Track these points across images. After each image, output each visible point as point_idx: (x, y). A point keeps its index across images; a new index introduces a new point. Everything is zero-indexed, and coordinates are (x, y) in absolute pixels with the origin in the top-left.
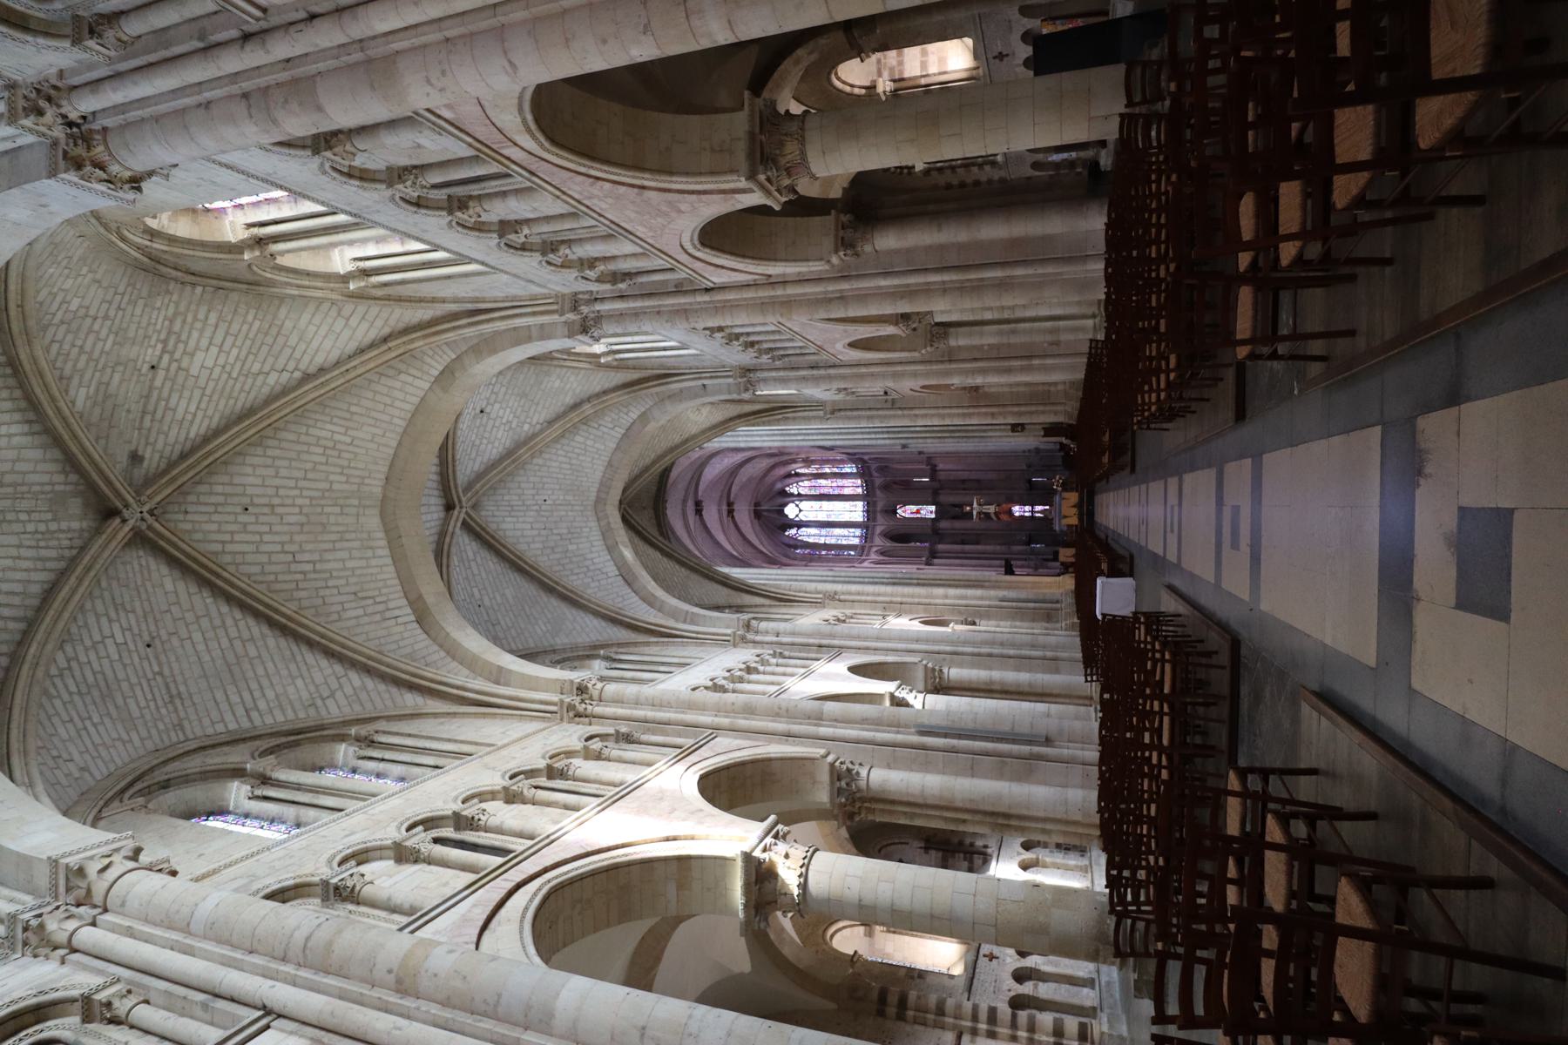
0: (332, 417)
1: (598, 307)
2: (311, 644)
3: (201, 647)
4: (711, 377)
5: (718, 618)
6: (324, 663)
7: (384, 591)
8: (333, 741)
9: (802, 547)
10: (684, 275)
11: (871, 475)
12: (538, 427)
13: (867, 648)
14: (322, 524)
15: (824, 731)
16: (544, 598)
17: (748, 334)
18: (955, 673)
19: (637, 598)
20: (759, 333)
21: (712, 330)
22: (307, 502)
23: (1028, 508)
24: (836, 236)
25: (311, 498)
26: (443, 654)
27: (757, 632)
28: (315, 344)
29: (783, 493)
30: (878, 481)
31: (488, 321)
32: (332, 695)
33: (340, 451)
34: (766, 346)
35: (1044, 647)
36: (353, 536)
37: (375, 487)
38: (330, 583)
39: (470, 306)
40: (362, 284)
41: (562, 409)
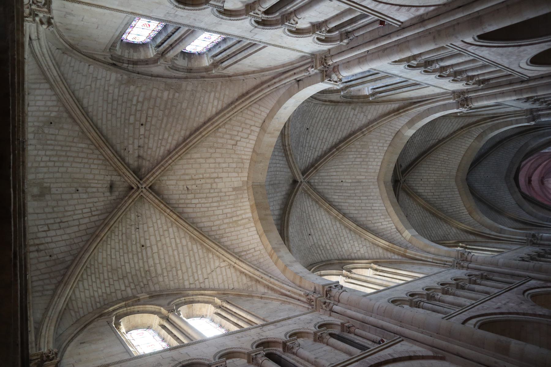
3: (416, 218)
6: (445, 225)
22: (436, 177)
25: (437, 176)
26: (479, 224)
28: (442, 132)
31: (498, 120)
33: (445, 162)
37: (454, 172)
38: (444, 201)
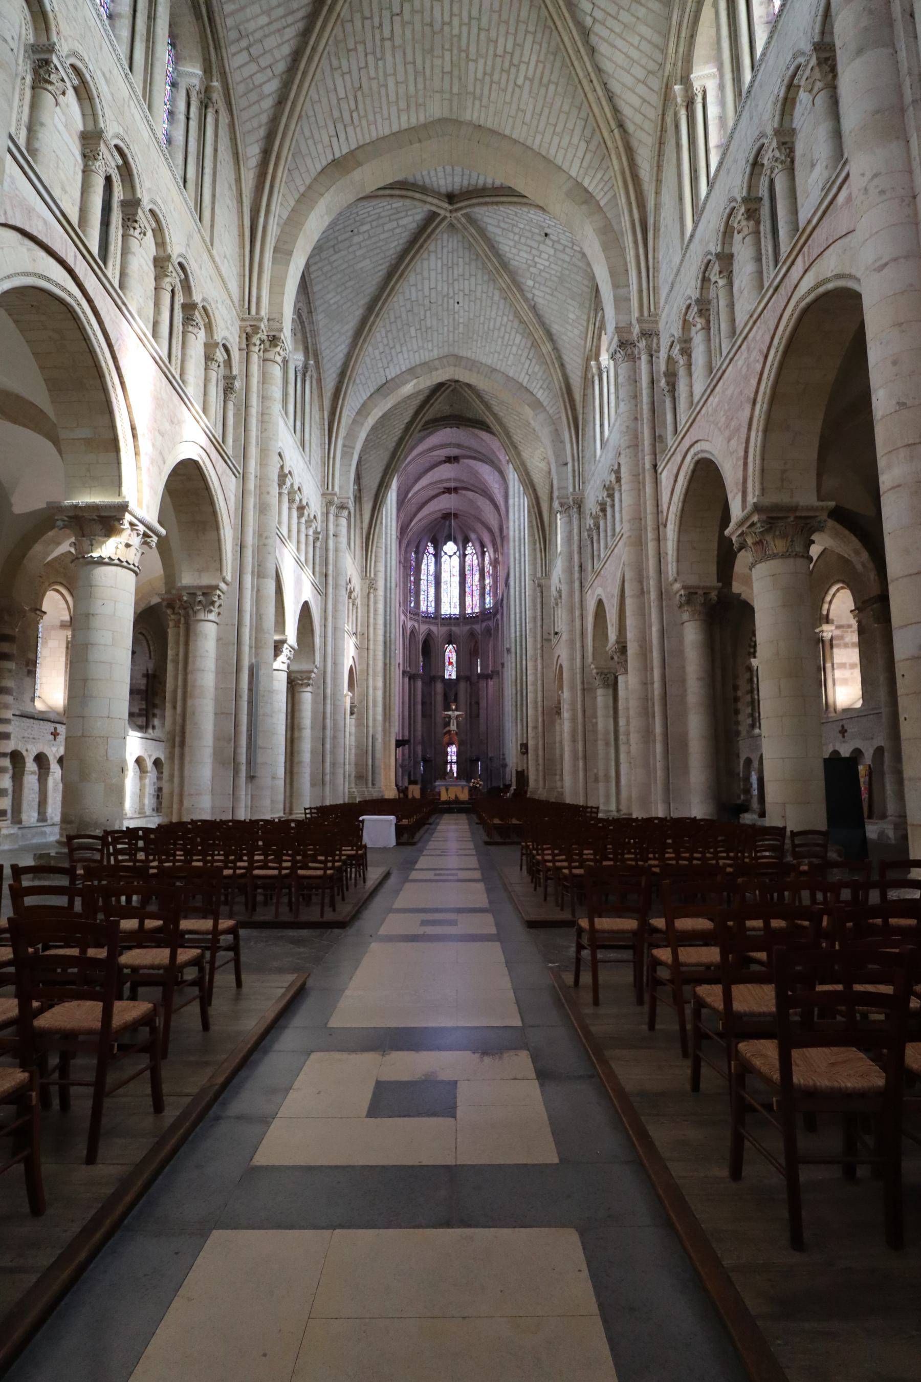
0: (543, 63)
1: (644, 358)
2: (306, 33)
4: (574, 471)
5: (349, 478)
6: (286, 50)
7: (364, 123)
8: (204, 60)
9: (417, 558)
10: (670, 444)
11: (482, 621)
12: (530, 296)
13: (326, 619)
14: (432, 50)
15: (248, 580)
16: (363, 301)
17: (613, 506)
18: (307, 697)
19: (365, 398)
20: (613, 517)
21: (618, 472)
23: (454, 758)
24: (698, 587)
25: (459, 36)
26: (302, 189)
27: (337, 516)
28: (619, 43)
29: (466, 540)
30: (477, 627)
31: (636, 242)
32: (253, 59)
33: (508, 72)
34: (602, 523)
35: (333, 773)
36: (420, 86)
37: (472, 113)
38: (370, 58)
39: (651, 221)
40: (679, 100)
41: (547, 322)
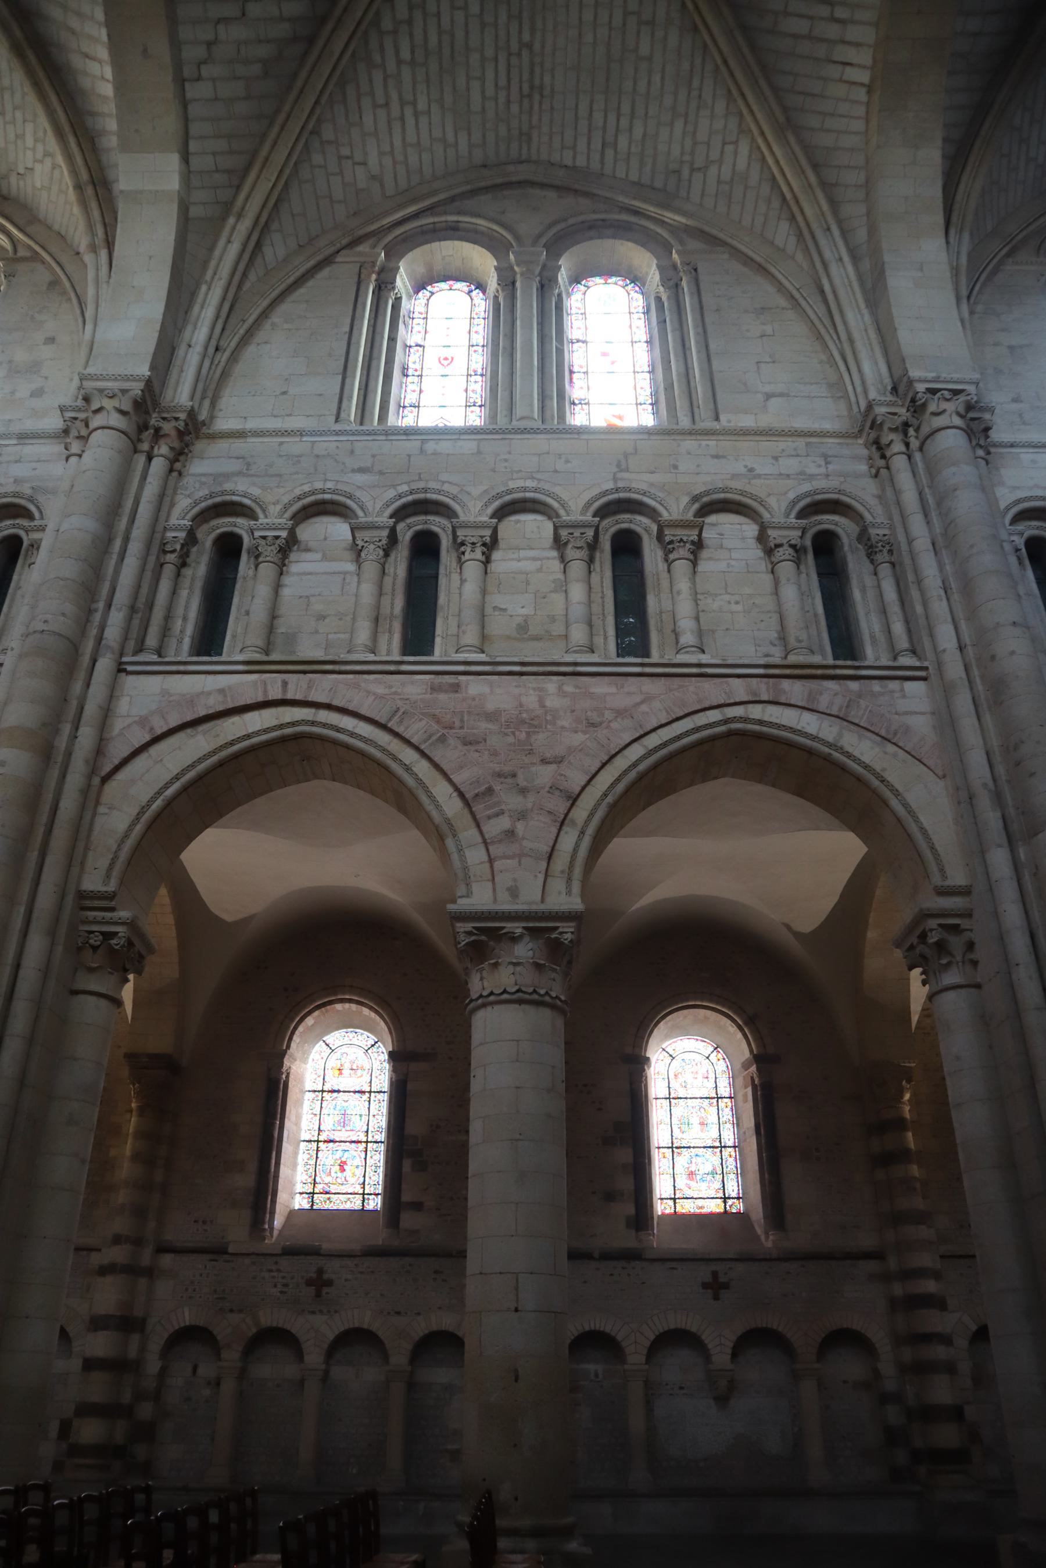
6: (720, 106)
32: (704, 169)
